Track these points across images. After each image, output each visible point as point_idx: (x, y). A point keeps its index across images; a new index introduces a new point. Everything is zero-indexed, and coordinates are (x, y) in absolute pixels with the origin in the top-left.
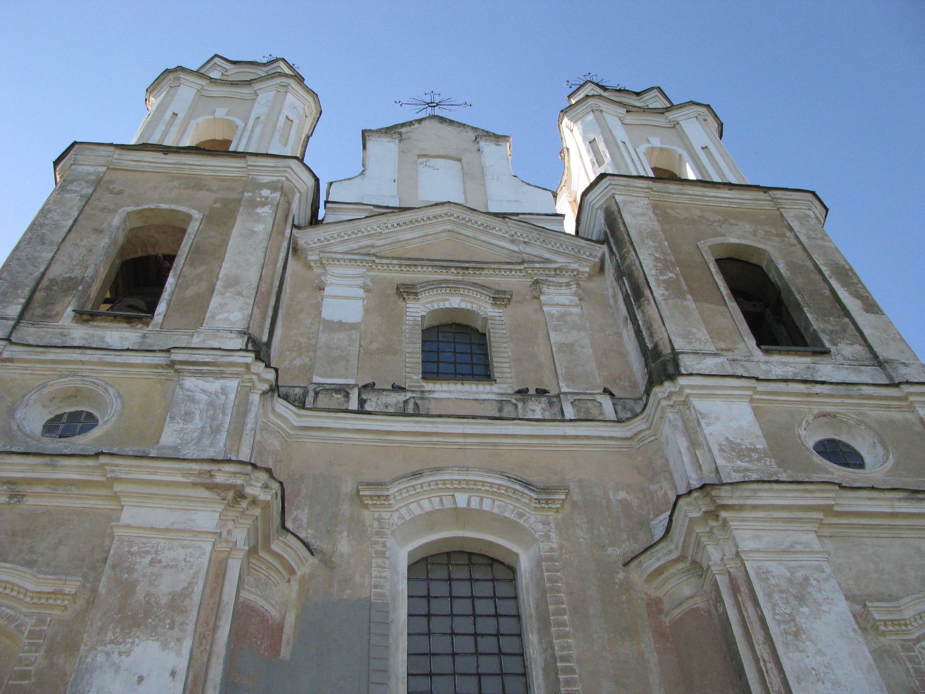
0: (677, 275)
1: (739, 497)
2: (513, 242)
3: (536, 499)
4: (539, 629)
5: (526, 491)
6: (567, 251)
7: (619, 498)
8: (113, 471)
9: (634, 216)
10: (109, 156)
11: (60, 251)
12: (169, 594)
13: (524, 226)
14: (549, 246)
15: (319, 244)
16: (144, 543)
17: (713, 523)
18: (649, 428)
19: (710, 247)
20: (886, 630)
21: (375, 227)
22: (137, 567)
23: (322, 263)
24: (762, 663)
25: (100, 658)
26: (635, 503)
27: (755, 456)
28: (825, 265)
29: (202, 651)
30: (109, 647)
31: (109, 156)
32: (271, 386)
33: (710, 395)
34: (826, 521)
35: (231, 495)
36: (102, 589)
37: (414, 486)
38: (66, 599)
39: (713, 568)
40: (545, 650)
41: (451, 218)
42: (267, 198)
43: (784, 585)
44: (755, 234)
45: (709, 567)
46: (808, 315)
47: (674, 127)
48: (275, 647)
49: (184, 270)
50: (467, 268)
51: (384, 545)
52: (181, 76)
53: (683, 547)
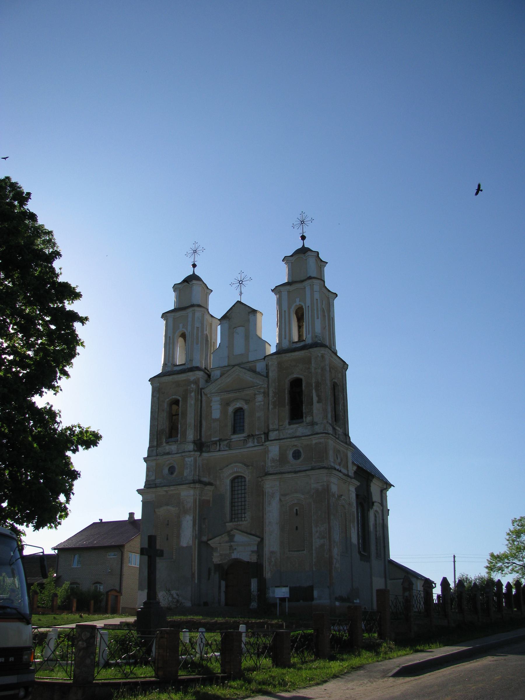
27: (276, 461)
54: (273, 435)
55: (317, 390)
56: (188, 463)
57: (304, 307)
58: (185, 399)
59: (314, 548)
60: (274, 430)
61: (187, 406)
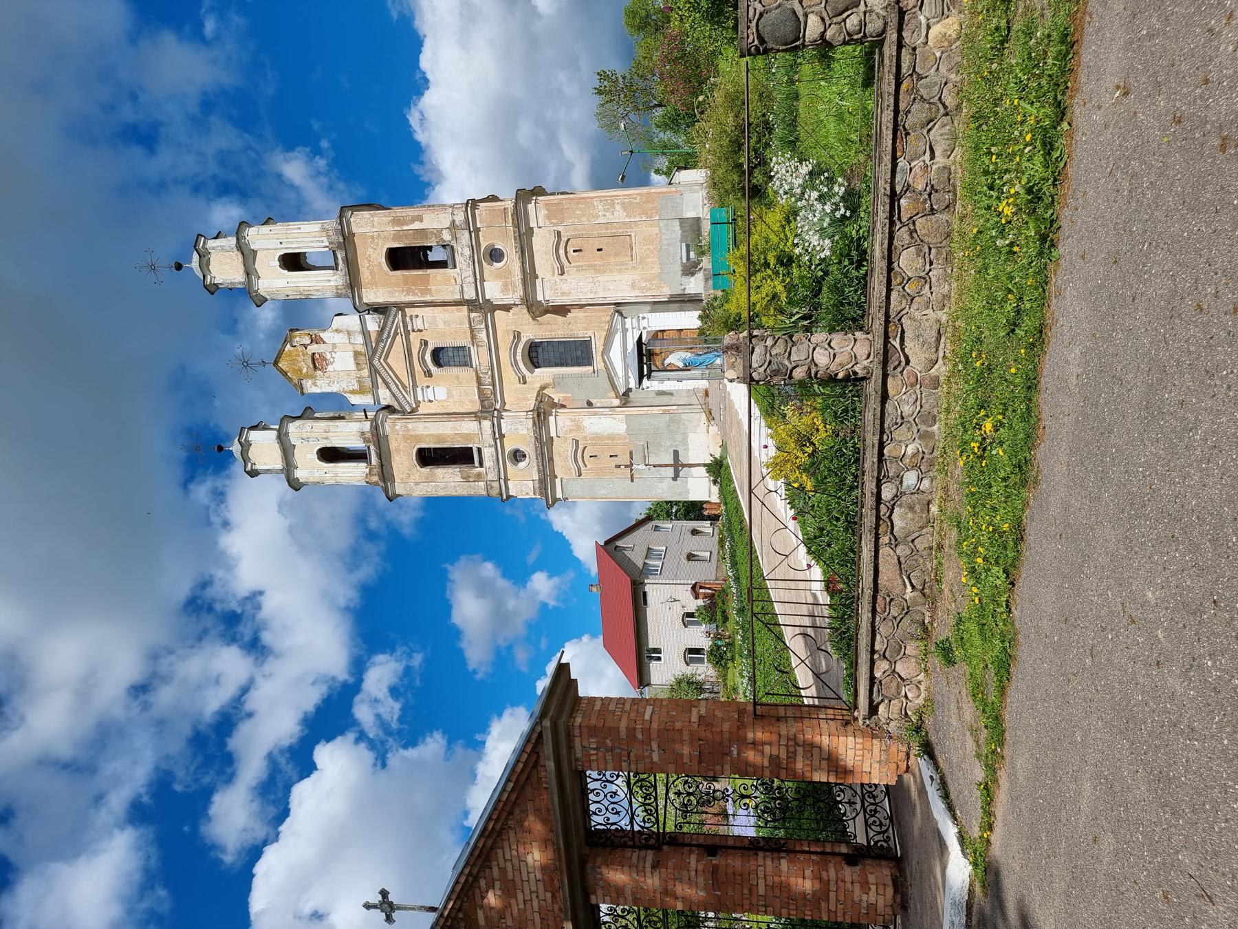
54: (470, 294)
55: (405, 223)
56: (509, 427)
57: (282, 252)
58: (417, 438)
59: (627, 220)
60: (462, 292)
61: (427, 435)
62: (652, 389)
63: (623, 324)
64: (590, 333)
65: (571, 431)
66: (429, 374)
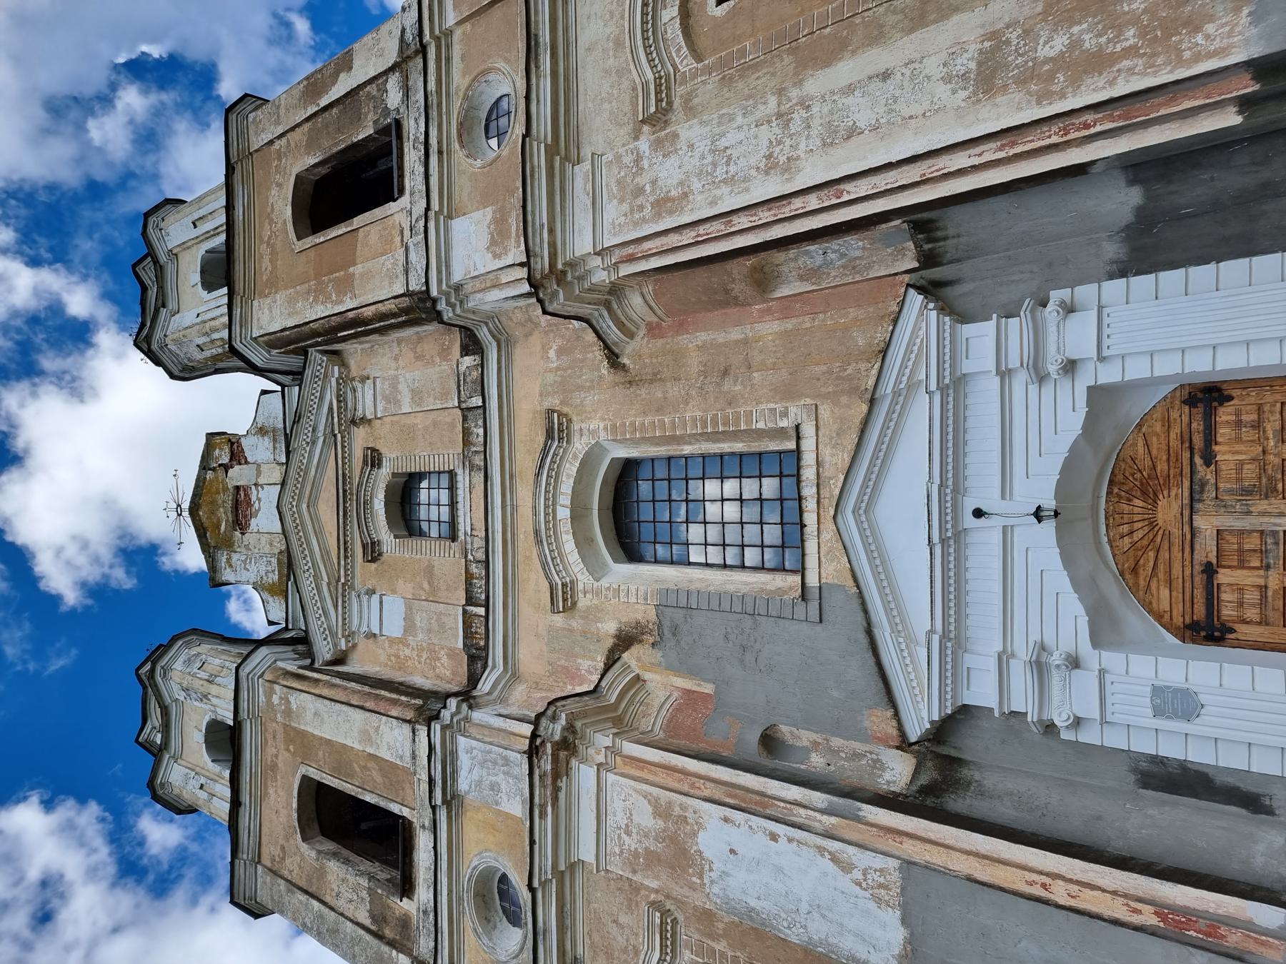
0: (330, 281)
1: (542, 248)
2: (314, 443)
3: (559, 442)
4: (678, 444)
5: (552, 451)
6: (319, 389)
7: (555, 358)
8: (546, 873)
9: (272, 320)
10: (245, 863)
11: (345, 913)
12: (655, 818)
13: (297, 431)
14: (315, 406)
15: (329, 639)
16: (611, 840)
17: (569, 278)
18: (487, 324)
19: (299, 239)
20: (665, 100)
21: (308, 582)
22: (633, 849)
23: (349, 636)
24: (700, 239)
25: (716, 889)
26: (559, 342)
28: (305, 108)
29: (706, 788)
30: (705, 881)
31: (245, 863)
32: (463, 701)
33: (446, 262)
34: (563, 153)
35: (563, 754)
36: (654, 884)
37: (553, 559)
38: (666, 920)
39: (613, 279)
40: (697, 440)
41: (294, 503)
42: (281, 698)
43: (625, 207)
44: (280, 185)
45: (611, 282)
46: (360, 137)
47: (176, 255)
48: (705, 697)
49: (357, 784)
50: (345, 491)
51: (608, 589)
52: (159, 782)
53: (595, 304)
62: (1115, 740)
63: (951, 354)
64: (796, 412)
65: (652, 859)
66: (373, 552)
